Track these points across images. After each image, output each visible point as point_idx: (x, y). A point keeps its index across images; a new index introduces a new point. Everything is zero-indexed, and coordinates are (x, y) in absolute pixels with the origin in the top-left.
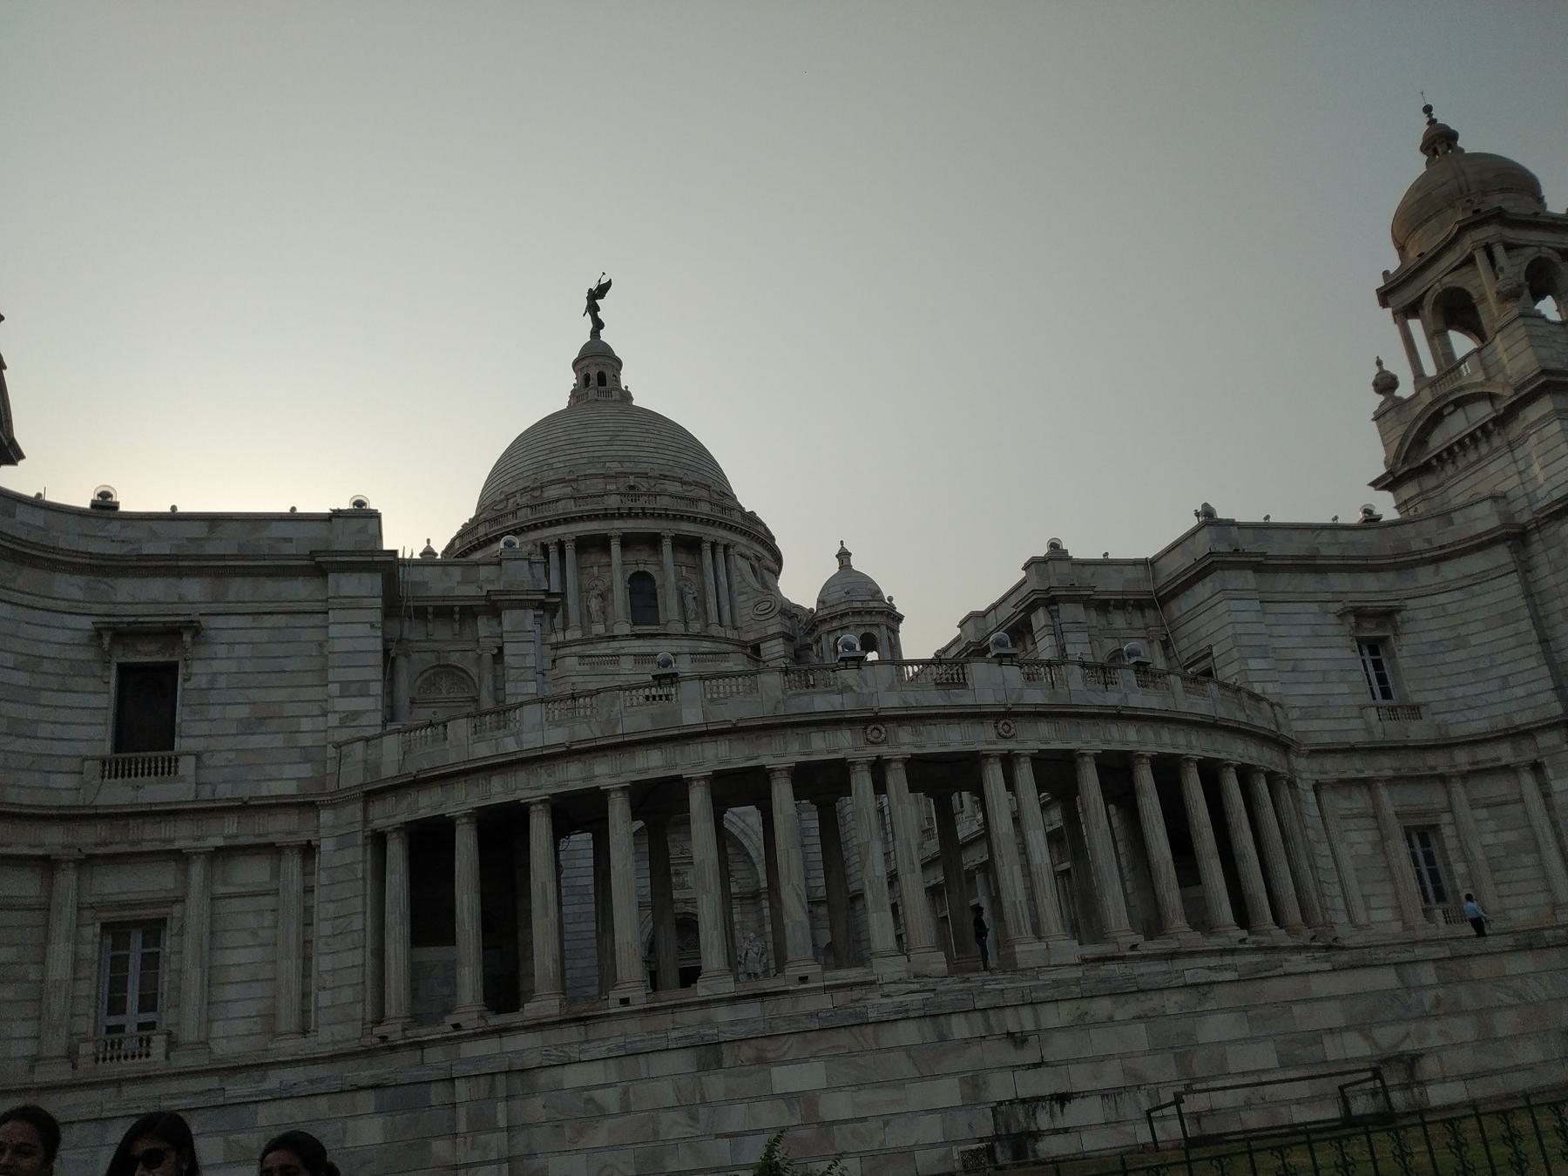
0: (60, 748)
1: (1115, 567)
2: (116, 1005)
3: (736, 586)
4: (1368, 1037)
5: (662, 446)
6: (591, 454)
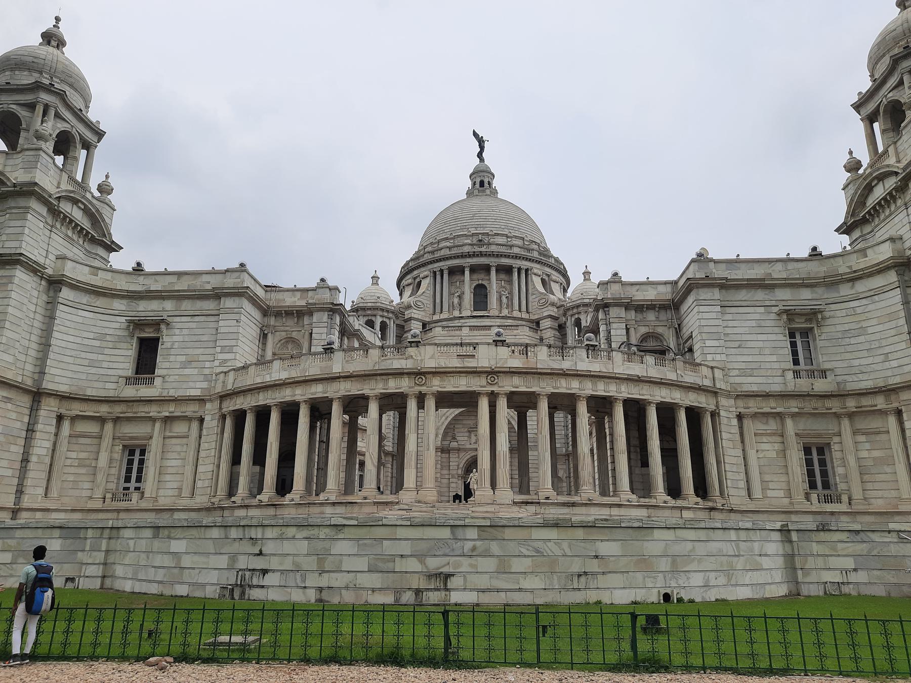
0: (110, 372)
1: (653, 286)
2: (128, 479)
3: (530, 291)
4: (422, 562)
5: (499, 218)
6: (462, 224)
